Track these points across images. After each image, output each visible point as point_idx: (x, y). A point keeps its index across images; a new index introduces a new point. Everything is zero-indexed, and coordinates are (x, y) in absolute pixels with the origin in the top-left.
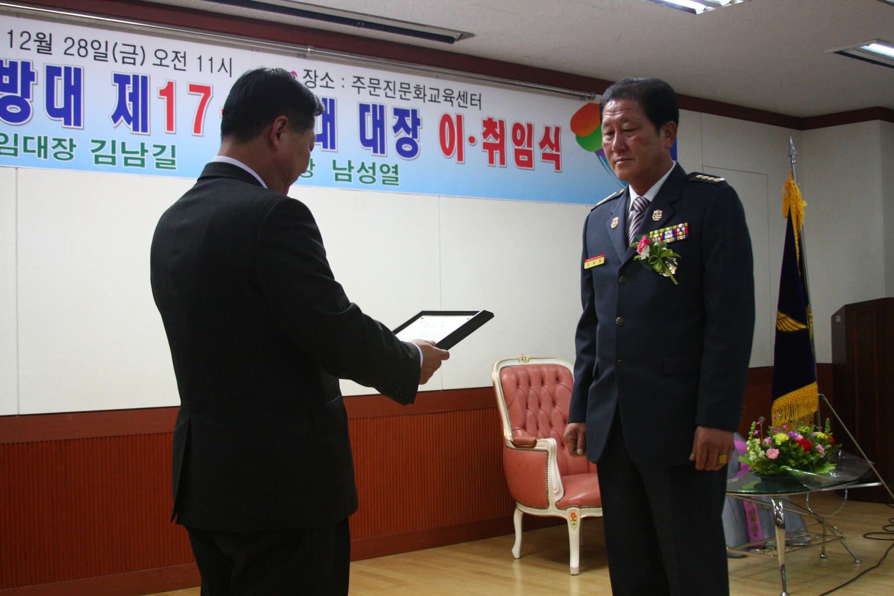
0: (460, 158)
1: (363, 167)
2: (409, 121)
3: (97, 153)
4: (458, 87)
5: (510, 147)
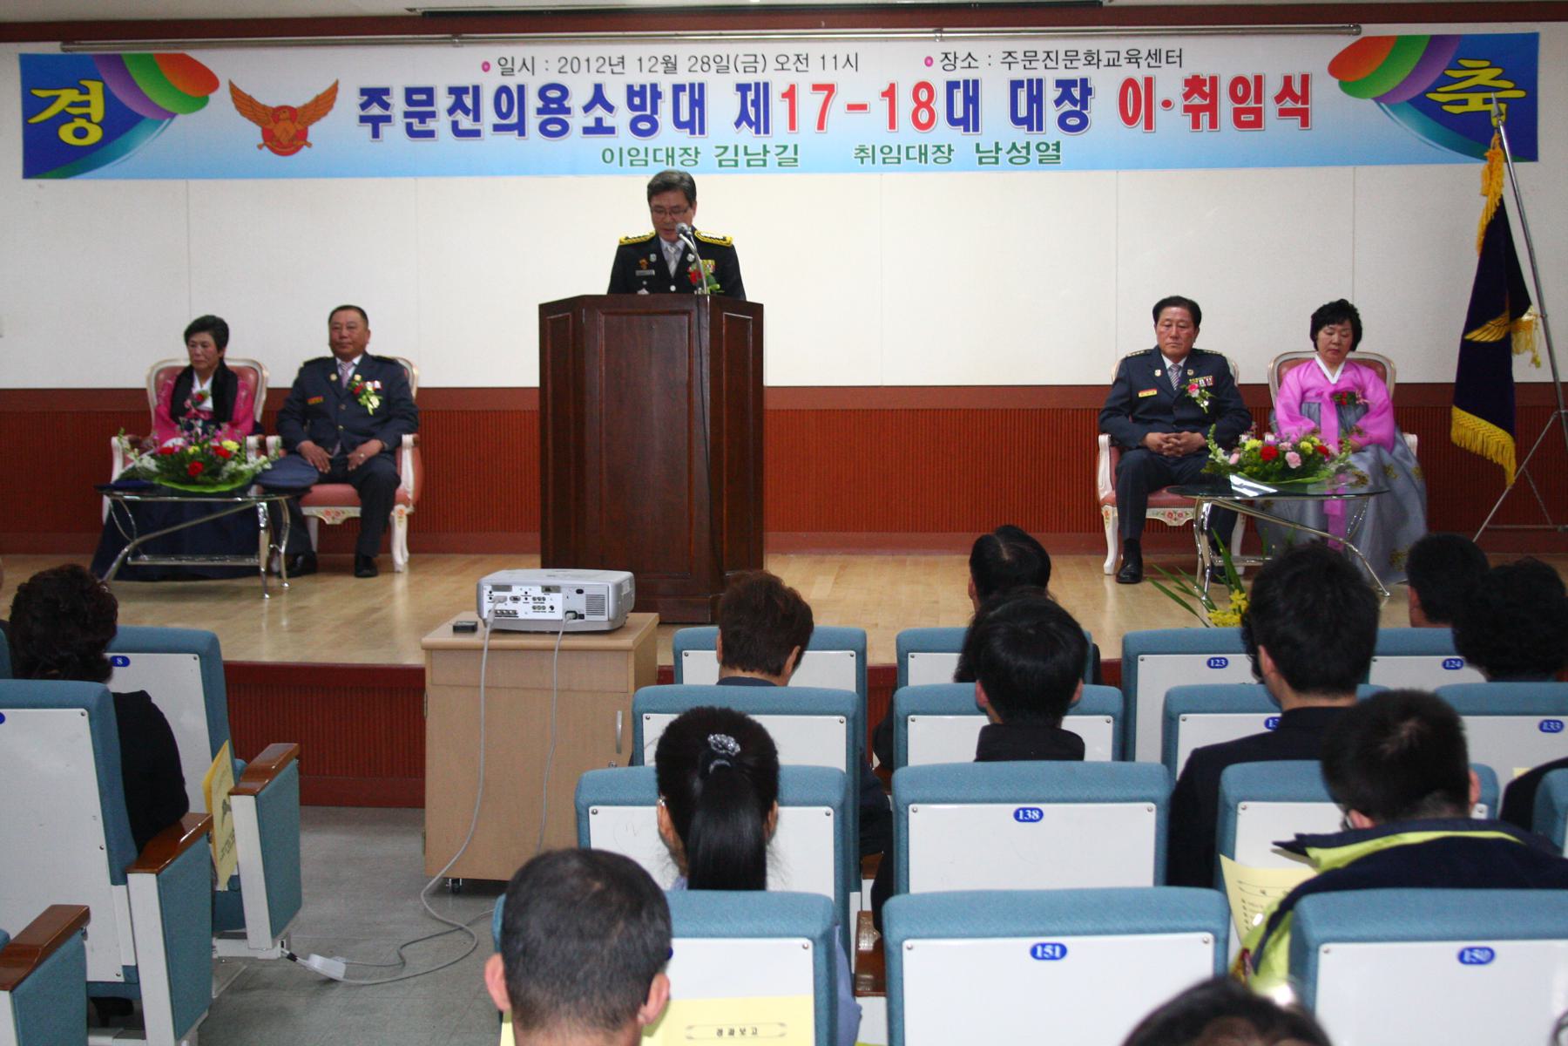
0: (1149, 125)
1: (1014, 146)
2: (1076, 93)
3: (720, 158)
4: (1145, 45)
5: (1226, 106)
